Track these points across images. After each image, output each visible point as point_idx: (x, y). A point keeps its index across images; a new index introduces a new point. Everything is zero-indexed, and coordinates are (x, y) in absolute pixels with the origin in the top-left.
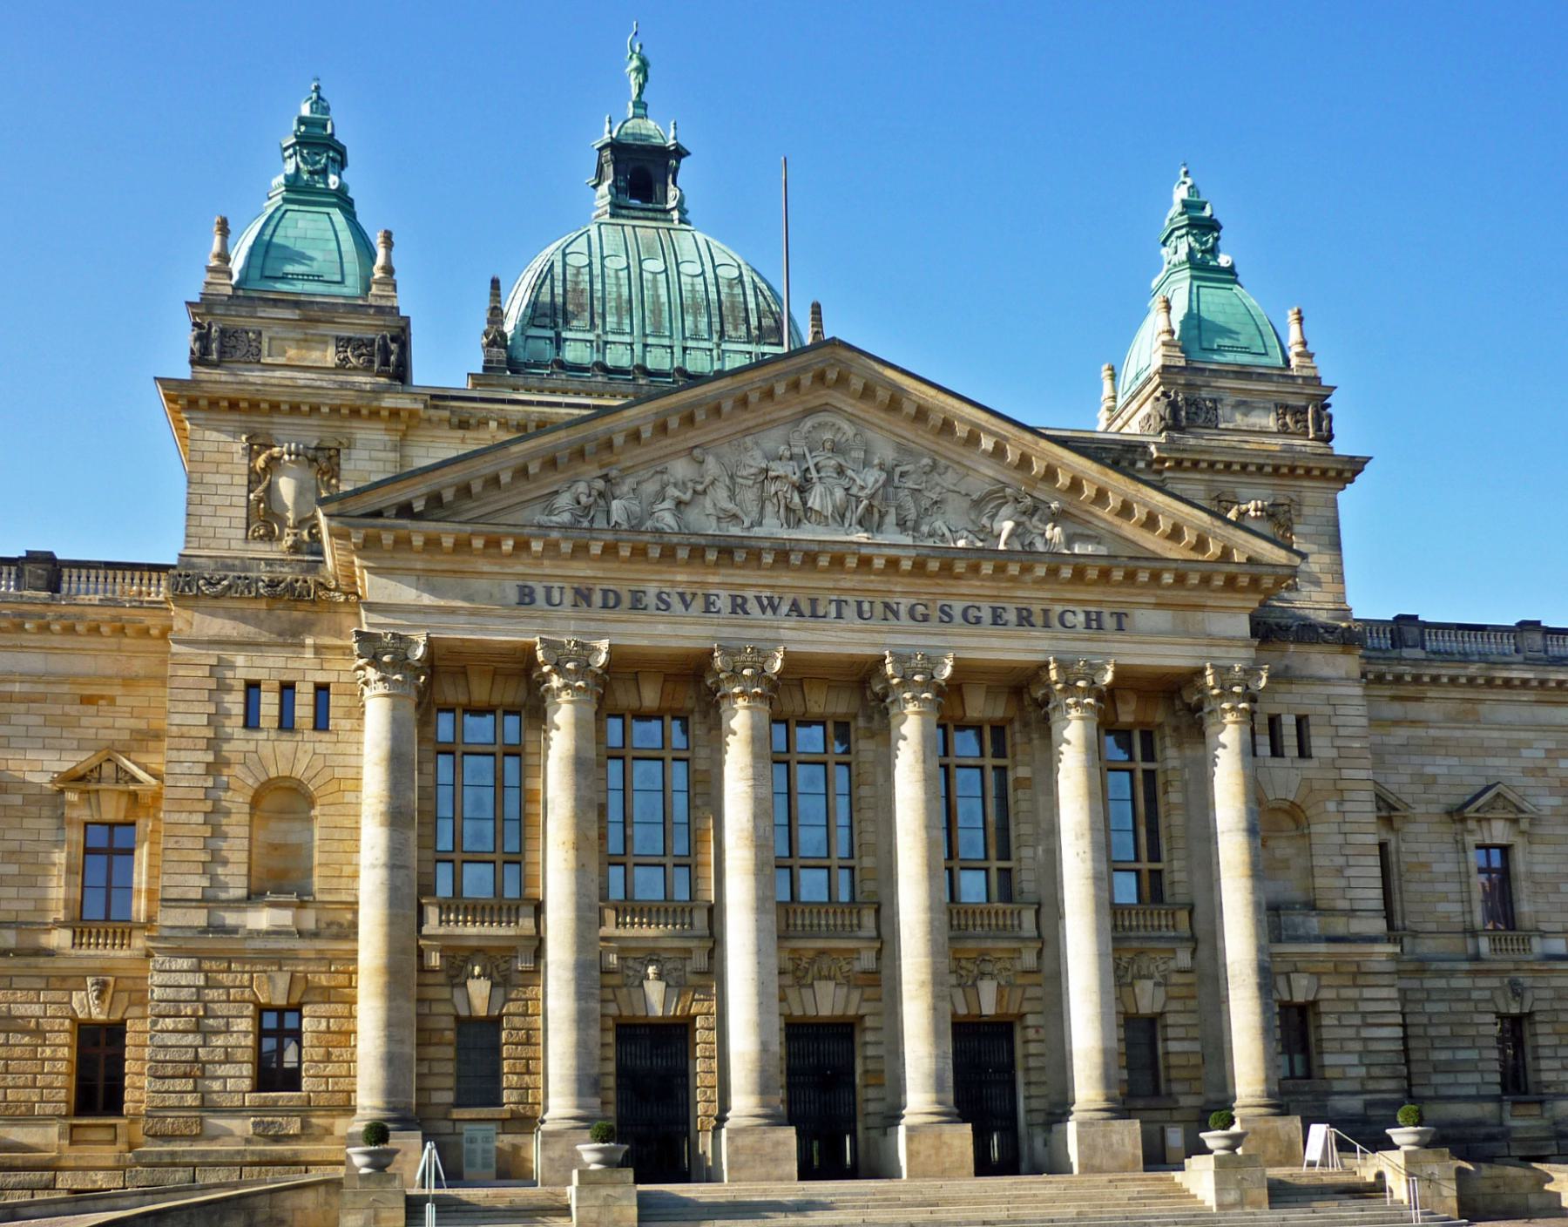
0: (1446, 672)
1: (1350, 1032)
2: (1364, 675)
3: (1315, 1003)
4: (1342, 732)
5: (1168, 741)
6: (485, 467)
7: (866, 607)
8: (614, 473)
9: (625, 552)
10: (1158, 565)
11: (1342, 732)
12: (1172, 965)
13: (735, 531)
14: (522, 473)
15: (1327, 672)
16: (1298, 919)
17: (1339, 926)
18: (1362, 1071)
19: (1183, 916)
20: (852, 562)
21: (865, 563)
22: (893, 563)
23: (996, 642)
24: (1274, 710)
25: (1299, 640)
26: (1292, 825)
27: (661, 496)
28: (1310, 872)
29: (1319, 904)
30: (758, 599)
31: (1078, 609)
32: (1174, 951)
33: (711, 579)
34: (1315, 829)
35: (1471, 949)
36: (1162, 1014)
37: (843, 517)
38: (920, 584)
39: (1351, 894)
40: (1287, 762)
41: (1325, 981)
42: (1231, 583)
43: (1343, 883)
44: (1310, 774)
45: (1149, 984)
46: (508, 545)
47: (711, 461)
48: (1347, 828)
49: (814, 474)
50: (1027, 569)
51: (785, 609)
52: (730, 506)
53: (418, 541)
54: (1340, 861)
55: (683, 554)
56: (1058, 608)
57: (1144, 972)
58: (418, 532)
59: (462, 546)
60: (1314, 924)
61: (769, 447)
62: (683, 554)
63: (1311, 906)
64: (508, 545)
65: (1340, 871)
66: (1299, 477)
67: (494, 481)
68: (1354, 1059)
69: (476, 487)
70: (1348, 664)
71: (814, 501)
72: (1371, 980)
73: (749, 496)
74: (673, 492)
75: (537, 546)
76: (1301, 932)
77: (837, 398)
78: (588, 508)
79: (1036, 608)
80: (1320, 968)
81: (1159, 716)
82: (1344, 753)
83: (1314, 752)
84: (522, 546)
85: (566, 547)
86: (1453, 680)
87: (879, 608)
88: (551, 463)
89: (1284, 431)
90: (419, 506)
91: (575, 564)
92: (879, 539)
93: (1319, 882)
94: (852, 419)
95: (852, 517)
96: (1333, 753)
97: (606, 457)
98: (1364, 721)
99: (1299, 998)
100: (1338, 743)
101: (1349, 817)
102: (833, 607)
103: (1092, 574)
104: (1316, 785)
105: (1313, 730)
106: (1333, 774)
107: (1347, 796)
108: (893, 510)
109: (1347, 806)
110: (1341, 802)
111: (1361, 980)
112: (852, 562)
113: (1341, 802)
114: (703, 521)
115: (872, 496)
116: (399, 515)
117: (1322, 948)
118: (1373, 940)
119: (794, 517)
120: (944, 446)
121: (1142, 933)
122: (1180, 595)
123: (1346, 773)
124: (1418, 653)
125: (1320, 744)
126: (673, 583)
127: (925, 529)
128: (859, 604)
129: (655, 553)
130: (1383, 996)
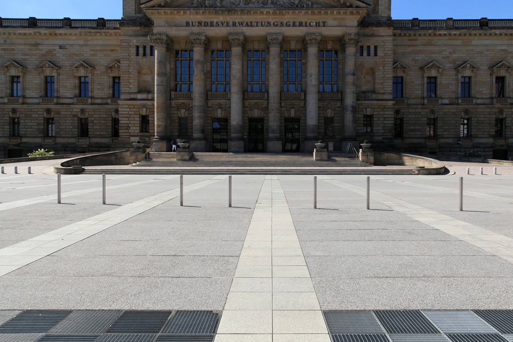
1: (381, 122)
3: (373, 115)
4: (386, 49)
11: (386, 49)
15: (383, 34)
17: (381, 97)
18: (383, 131)
19: (340, 94)
24: (368, 44)
28: (374, 84)
34: (376, 73)
36: (334, 117)
40: (371, 57)
45: (331, 110)
48: (385, 73)
54: (382, 81)
60: (374, 96)
63: (374, 92)
65: (382, 83)
68: (381, 128)
83: (378, 55)
93: (376, 86)
96: (383, 55)
98: (392, 46)
99: (368, 114)
100: (384, 52)
105: (378, 49)
107: (385, 65)
110: (383, 67)
111: (384, 110)
113: (383, 67)
117: (375, 102)
125: (380, 53)
130: (390, 113)
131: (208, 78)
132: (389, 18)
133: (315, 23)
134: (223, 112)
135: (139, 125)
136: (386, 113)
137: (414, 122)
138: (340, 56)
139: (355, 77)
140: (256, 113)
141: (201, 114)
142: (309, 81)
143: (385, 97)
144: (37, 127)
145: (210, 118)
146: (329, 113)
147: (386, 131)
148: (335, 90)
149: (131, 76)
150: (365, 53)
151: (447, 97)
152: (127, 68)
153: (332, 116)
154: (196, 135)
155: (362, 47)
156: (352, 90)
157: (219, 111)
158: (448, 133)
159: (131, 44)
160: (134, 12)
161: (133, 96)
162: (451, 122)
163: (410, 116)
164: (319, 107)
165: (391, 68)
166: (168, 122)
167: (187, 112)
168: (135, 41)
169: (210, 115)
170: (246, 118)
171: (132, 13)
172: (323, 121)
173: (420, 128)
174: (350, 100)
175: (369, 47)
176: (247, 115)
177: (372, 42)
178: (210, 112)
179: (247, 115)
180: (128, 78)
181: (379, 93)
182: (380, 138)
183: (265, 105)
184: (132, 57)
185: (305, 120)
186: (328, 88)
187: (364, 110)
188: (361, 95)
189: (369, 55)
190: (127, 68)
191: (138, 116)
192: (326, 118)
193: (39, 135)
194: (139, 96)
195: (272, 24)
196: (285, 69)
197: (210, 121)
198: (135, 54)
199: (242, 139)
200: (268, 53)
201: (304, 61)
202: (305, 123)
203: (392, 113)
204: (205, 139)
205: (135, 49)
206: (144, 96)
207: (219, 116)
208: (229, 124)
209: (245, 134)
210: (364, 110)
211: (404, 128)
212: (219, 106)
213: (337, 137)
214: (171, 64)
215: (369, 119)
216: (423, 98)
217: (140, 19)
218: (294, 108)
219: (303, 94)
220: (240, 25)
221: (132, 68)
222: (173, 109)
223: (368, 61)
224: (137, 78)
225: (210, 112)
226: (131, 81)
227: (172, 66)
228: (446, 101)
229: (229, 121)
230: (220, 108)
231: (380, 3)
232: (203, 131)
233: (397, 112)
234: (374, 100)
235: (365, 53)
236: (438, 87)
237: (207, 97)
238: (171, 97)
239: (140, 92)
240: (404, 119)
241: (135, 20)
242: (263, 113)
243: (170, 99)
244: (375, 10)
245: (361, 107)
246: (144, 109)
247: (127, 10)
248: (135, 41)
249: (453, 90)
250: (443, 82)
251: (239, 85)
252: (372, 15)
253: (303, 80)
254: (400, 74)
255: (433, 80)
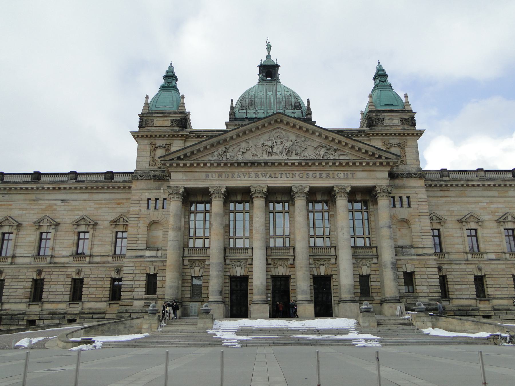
0: (454, 183)
1: (424, 280)
2: (425, 185)
3: (414, 272)
5: (370, 204)
6: (197, 147)
7: (288, 174)
8: (227, 147)
9: (229, 165)
10: (361, 161)
12: (372, 262)
13: (256, 158)
14: (205, 148)
16: (408, 250)
17: (420, 252)
18: (428, 291)
19: (374, 249)
20: (283, 164)
21: (286, 164)
22: (293, 164)
23: (321, 182)
25: (407, 177)
26: (407, 225)
27: (239, 151)
28: (412, 237)
29: (414, 246)
30: (262, 174)
31: (342, 173)
32: (372, 258)
33: (250, 170)
34: (412, 226)
35: (466, 258)
37: (282, 153)
38: (301, 169)
39: (423, 243)
40: (404, 208)
41: (416, 266)
42: (381, 164)
43: (421, 240)
44: (410, 211)
45: (366, 267)
46: (202, 165)
47: (250, 142)
49: (275, 144)
50: (327, 164)
51: (268, 176)
52: (255, 153)
53: (181, 165)
54: (420, 234)
55: (242, 165)
56: (336, 173)
57: (364, 263)
58: (181, 163)
59: (192, 165)
60: (413, 251)
61: (265, 138)
62: (242, 165)
63: (412, 246)
64: (202, 165)
65: (420, 237)
66: (406, 136)
67: (199, 150)
69: (195, 152)
70: (422, 183)
71: (275, 151)
72: (429, 266)
73: (260, 150)
74: (241, 150)
75: (209, 165)
76: (409, 253)
77: (281, 126)
78: (221, 155)
79: (331, 173)
80: (414, 262)
81: (368, 198)
82: (420, 206)
84: (205, 164)
85: (215, 165)
86: (457, 185)
87: (291, 175)
88: (212, 145)
89: (402, 124)
90: (182, 157)
91: (218, 168)
92: (290, 158)
94: (285, 130)
95: (284, 153)
96: (417, 206)
97: (226, 143)
98: (426, 197)
99: (409, 271)
101: (422, 223)
102: (280, 175)
103: (344, 164)
104: (413, 214)
105: (411, 200)
106: (418, 211)
108: (294, 151)
109: (421, 220)
111: (426, 266)
112: (283, 164)
114: (249, 157)
115: (289, 148)
116: (177, 160)
117: (415, 257)
118: (430, 255)
119: (270, 154)
120: (307, 135)
121: (363, 254)
122: (368, 168)
123: (421, 211)
124: (448, 178)
125: (413, 203)
126: (241, 171)
127: (302, 155)
128: (286, 174)
129: (236, 165)
131: (225, 232)
132: (419, 169)
133: (343, 175)
134: (243, 270)
135: (144, 286)
136: (429, 269)
137: (459, 280)
138: (371, 208)
139: (392, 230)
140: (281, 271)
141: (220, 273)
142: (340, 234)
143: (425, 251)
144: (23, 290)
145: (228, 277)
146: (365, 271)
147: (432, 291)
148: (368, 244)
149: (139, 230)
150: (398, 204)
151: (492, 251)
152: (137, 222)
153: (368, 274)
154: (211, 298)
155: (393, 198)
156: (390, 244)
157: (239, 269)
158: (500, 293)
159: (142, 197)
160: (148, 165)
161: (140, 253)
162: (501, 279)
163: (454, 273)
164: (353, 264)
165: (429, 220)
166: (180, 282)
167: (202, 270)
168: (147, 194)
169: (228, 274)
170: (270, 277)
171: (146, 166)
172: (358, 280)
173: (468, 286)
174: (387, 255)
175: (401, 198)
176: (270, 273)
177: (404, 193)
178: (227, 270)
179: (270, 273)
180: (137, 233)
181: (418, 248)
182: (426, 300)
183: (291, 261)
184: (142, 210)
185: (339, 278)
186: (360, 242)
187: (404, 266)
188: (399, 250)
189: (402, 206)
190: (137, 222)
191: (145, 275)
192: (361, 277)
193: (24, 300)
194: (148, 253)
195: (297, 175)
196: (311, 222)
197: (228, 281)
198: (146, 208)
199: (266, 302)
200: (294, 205)
201: (332, 213)
202: (339, 282)
203: (436, 269)
204: (223, 302)
205: (146, 202)
206: (153, 253)
207: (239, 275)
208: (249, 284)
209: (269, 295)
210: (404, 266)
211: (449, 286)
212: (239, 263)
213: (376, 298)
214: (185, 218)
215: (409, 278)
216: (466, 253)
217: (154, 171)
218: (323, 265)
219: (333, 250)
220: (263, 177)
221: (141, 222)
222: (186, 267)
223: (403, 213)
224: (146, 233)
225: (227, 270)
226: (139, 236)
227: (187, 220)
228: (493, 256)
229: (250, 281)
230: (240, 265)
231: (406, 154)
232: (221, 293)
233: (440, 269)
234: (414, 255)
235: (398, 204)
236: (481, 240)
237: (225, 253)
238: (184, 254)
239: (148, 248)
240: (448, 277)
241: (149, 173)
242: (288, 270)
243: (183, 257)
244: (404, 163)
245: (399, 262)
246: (152, 268)
247: (141, 163)
248: (147, 194)
249: (499, 243)
250: (485, 235)
251: (263, 239)
252: (400, 166)
253: (332, 233)
254: (437, 226)
255: (473, 232)
